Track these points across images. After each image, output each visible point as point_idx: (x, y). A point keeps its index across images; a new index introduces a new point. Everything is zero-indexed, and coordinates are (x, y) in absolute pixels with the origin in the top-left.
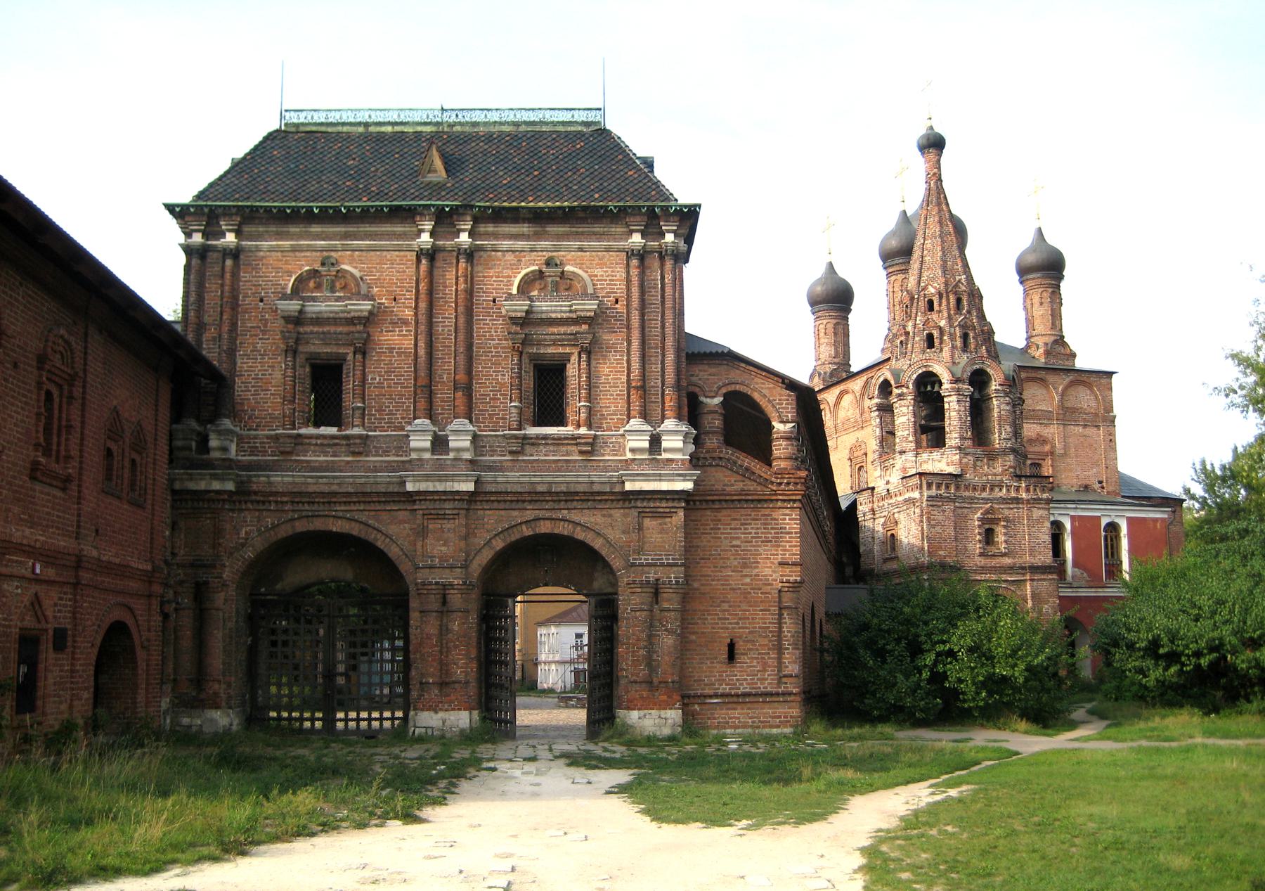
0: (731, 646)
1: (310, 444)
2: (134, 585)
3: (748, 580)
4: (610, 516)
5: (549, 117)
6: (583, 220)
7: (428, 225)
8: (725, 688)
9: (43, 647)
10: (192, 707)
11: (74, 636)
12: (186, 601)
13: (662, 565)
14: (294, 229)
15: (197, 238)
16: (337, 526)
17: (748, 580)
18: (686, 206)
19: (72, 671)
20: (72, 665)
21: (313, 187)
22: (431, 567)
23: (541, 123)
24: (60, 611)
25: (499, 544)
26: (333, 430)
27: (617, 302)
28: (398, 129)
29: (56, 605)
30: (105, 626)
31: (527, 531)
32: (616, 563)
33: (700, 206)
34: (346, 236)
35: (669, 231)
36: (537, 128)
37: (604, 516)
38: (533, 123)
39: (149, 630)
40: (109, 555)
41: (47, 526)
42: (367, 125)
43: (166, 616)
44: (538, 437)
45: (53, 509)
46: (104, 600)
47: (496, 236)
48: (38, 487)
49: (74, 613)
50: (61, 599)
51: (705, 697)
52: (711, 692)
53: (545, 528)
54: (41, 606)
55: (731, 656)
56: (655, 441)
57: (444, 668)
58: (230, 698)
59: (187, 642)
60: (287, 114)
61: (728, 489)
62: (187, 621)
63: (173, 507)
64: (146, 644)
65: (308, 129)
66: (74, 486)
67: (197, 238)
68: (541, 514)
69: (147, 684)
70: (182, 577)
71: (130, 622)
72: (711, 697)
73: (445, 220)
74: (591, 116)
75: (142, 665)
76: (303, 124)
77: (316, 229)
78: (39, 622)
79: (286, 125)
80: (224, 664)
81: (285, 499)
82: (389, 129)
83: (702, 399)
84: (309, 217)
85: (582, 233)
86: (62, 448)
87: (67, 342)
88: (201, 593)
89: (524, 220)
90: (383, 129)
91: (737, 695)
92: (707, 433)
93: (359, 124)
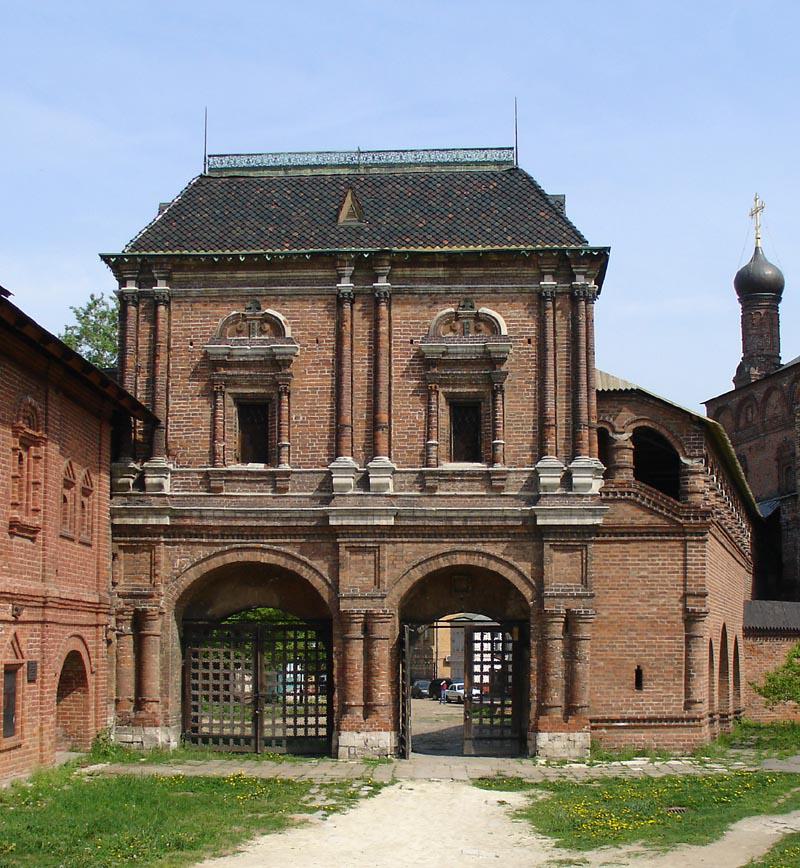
0: (639, 673)
1: (238, 481)
2: (85, 617)
3: (655, 609)
4: (523, 548)
5: (461, 156)
6: (497, 264)
7: (348, 270)
8: (632, 713)
9: (20, 679)
10: (134, 725)
11: (42, 667)
12: (127, 628)
13: (572, 596)
14: (221, 275)
15: (131, 287)
16: (265, 558)
17: (655, 609)
18: (595, 250)
19: (42, 699)
20: (42, 693)
21: (238, 232)
22: (353, 598)
23: (456, 163)
24: (31, 647)
25: (417, 575)
26: (260, 467)
27: (529, 342)
28: (317, 172)
29: (28, 641)
30: (64, 657)
31: (443, 563)
32: (528, 593)
33: (609, 249)
34: (270, 282)
35: (579, 273)
36: (452, 169)
37: (517, 548)
38: (448, 164)
39: (97, 657)
40: (67, 591)
41: (21, 573)
42: (286, 168)
43: (109, 642)
44: (455, 473)
45: (25, 556)
46: (63, 632)
47: (413, 280)
48: (16, 539)
49: (42, 647)
50: (32, 636)
51: (613, 721)
52: (618, 717)
53: (461, 560)
54: (18, 644)
55: (639, 684)
56: (567, 480)
57: (368, 694)
58: (167, 717)
59: (129, 666)
60: (211, 160)
61: (636, 522)
62: (128, 643)
63: (113, 541)
64: (94, 669)
65: (231, 174)
66: (40, 535)
67: (131, 287)
68: (458, 547)
69: (96, 705)
70: (122, 606)
71: (82, 650)
72: (618, 721)
73: (367, 266)
74: (504, 156)
75: (92, 688)
76: (226, 169)
77: (241, 275)
78: (17, 658)
79: (210, 170)
80: (161, 685)
81: (216, 532)
82: (308, 172)
83: (611, 434)
84: (235, 264)
85: (495, 276)
86: (31, 502)
87: (34, 408)
88: (140, 621)
89: (440, 264)
90: (304, 172)
91: (644, 720)
92: (619, 468)
93: (279, 168)
